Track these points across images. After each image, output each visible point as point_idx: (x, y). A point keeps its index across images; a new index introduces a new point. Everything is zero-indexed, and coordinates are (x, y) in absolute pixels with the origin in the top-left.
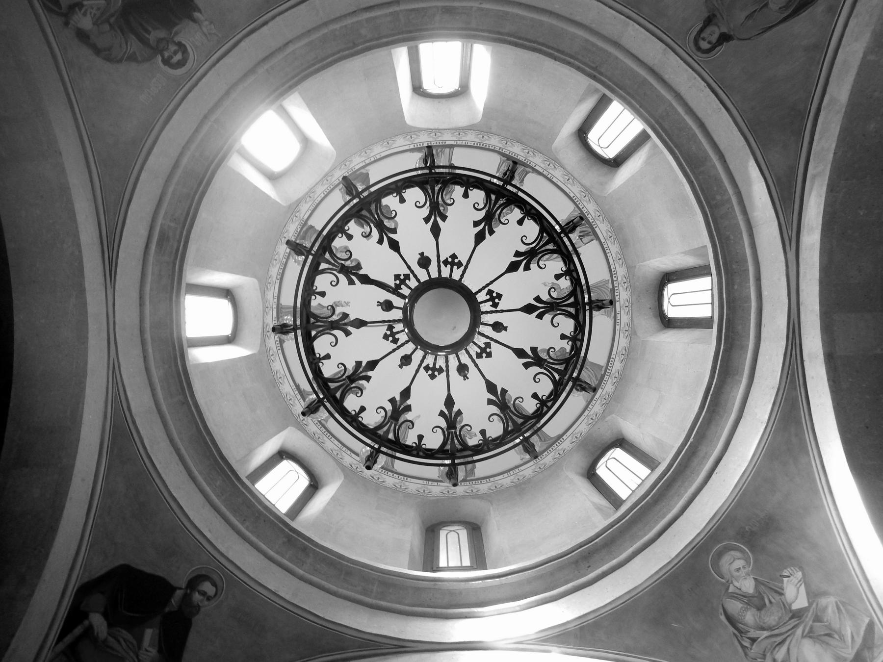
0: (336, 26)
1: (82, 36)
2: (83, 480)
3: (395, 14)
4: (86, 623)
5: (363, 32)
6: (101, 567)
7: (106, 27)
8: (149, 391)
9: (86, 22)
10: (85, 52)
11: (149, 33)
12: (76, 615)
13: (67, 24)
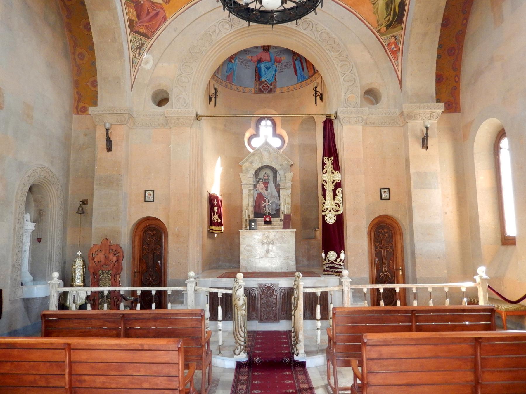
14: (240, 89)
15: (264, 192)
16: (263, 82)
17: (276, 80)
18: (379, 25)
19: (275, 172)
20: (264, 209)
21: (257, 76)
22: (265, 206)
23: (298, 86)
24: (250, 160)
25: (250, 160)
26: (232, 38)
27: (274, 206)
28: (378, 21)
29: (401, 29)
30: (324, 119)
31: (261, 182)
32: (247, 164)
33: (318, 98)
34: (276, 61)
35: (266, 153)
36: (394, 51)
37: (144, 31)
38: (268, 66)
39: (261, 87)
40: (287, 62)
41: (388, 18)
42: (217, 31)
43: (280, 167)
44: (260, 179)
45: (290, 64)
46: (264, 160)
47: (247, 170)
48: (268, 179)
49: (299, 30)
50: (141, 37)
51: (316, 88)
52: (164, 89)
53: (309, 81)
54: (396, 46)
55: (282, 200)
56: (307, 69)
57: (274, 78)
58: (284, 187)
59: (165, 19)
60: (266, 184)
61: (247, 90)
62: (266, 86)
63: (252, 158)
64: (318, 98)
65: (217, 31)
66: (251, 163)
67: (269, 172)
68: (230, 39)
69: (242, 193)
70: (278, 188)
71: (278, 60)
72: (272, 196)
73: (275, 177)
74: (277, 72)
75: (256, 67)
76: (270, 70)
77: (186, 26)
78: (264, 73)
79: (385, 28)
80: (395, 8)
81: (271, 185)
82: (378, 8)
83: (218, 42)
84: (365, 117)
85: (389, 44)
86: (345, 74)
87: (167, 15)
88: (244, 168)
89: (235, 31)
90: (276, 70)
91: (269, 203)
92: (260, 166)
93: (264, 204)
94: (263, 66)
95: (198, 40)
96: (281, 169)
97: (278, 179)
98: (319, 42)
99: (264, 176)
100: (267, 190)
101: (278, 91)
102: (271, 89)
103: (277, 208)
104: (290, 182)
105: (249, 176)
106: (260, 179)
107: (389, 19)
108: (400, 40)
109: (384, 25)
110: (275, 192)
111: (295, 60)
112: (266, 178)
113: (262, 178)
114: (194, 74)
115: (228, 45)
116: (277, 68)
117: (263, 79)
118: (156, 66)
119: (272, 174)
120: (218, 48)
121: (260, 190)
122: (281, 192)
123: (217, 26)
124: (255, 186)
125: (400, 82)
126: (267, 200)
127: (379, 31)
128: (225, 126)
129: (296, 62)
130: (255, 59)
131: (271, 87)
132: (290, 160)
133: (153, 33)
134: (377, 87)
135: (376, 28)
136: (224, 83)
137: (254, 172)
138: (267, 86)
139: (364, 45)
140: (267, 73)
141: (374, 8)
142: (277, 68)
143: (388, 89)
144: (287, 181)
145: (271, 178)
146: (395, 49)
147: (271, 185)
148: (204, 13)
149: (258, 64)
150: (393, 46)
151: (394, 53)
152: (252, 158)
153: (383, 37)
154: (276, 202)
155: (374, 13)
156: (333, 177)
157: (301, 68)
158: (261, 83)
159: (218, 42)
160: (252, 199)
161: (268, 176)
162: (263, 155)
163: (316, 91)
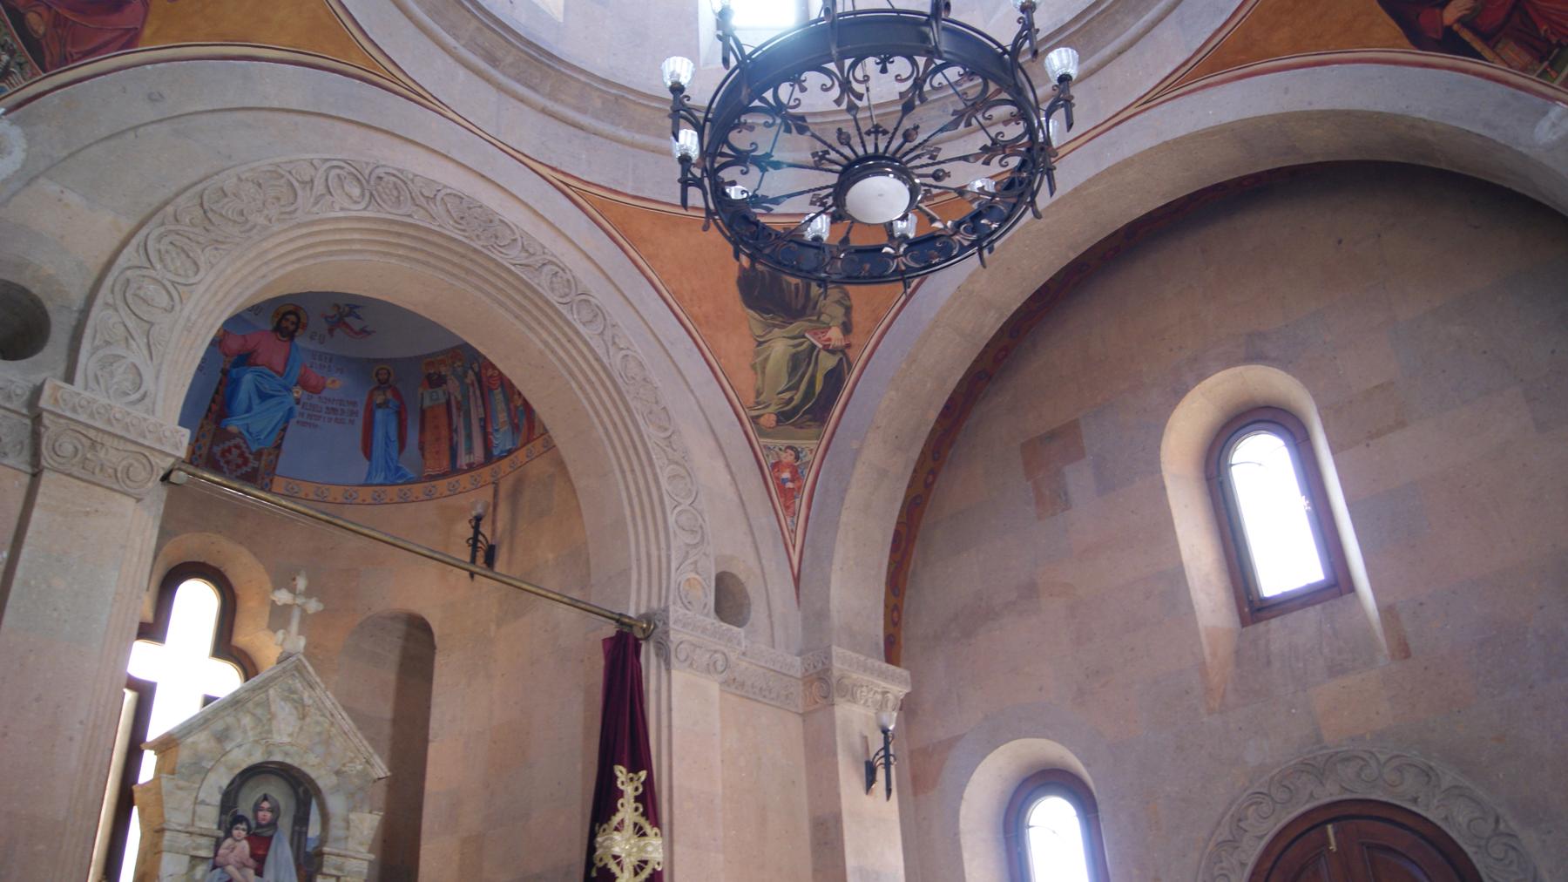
0: (623, 133)
1: (847, 328)
2: (1286, 91)
3: (552, 96)
4: (1456, 27)
5: (598, 103)
6: (1387, 26)
7: (824, 318)
8: (1156, 31)
9: (835, 335)
10: (856, 317)
11: (797, 286)
12: (1450, 43)
13: (848, 346)
16: (234, 436)
17: (278, 447)
18: (758, 403)
21: (216, 408)
23: (366, 493)
24: (219, 725)
26: (356, 236)
28: (759, 393)
29: (819, 437)
30: (610, 630)
31: (240, 831)
34: (303, 383)
35: (288, 707)
36: (785, 487)
37: (41, 30)
38: (267, 387)
39: (217, 450)
41: (787, 395)
42: (319, 187)
43: (334, 779)
44: (239, 819)
46: (277, 738)
48: (273, 824)
49: (569, 317)
50: (18, 44)
51: (478, 519)
52: (35, 291)
53: (418, 489)
54: (796, 475)
56: (422, 448)
57: (274, 437)
58: (340, 868)
59: (130, 40)
60: (260, 845)
62: (235, 452)
63: (230, 720)
65: (319, 187)
67: (278, 792)
68: (348, 236)
73: (301, 820)
74: (293, 421)
75: (225, 372)
77: (199, 108)
78: (244, 406)
79: (773, 418)
80: (813, 377)
81: (282, 852)
82: (766, 359)
83: (313, 223)
84: (733, 657)
85: (776, 466)
86: (680, 504)
87: (147, 32)
89: (375, 220)
90: (291, 410)
92: (258, 757)
94: (248, 380)
95: (240, 179)
96: (336, 789)
98: (619, 381)
99: (257, 808)
100: (259, 873)
101: (279, 484)
102: (255, 470)
104: (364, 849)
106: (239, 819)
107: (791, 399)
108: (809, 464)
109: (772, 408)
111: (379, 406)
112: (265, 816)
113: (249, 815)
114: (202, 288)
115: (331, 253)
116: (298, 408)
117: (234, 426)
118: (28, 184)
119: (292, 804)
120: (301, 243)
121: (231, 869)
123: (321, 171)
125: (797, 580)
127: (755, 420)
131: (253, 464)
133: (65, 61)
134: (742, 577)
135: (750, 408)
138: (242, 455)
139: (717, 440)
141: (757, 354)
142: (298, 408)
143: (770, 589)
144: (352, 844)
145: (285, 823)
146: (790, 485)
148: (276, 105)
149: (236, 365)
150: (786, 475)
151: (788, 496)
153: (763, 441)
155: (753, 367)
156: (642, 849)
158: (221, 434)
159: (313, 223)
161: (275, 810)
162: (273, 716)
163: (477, 532)
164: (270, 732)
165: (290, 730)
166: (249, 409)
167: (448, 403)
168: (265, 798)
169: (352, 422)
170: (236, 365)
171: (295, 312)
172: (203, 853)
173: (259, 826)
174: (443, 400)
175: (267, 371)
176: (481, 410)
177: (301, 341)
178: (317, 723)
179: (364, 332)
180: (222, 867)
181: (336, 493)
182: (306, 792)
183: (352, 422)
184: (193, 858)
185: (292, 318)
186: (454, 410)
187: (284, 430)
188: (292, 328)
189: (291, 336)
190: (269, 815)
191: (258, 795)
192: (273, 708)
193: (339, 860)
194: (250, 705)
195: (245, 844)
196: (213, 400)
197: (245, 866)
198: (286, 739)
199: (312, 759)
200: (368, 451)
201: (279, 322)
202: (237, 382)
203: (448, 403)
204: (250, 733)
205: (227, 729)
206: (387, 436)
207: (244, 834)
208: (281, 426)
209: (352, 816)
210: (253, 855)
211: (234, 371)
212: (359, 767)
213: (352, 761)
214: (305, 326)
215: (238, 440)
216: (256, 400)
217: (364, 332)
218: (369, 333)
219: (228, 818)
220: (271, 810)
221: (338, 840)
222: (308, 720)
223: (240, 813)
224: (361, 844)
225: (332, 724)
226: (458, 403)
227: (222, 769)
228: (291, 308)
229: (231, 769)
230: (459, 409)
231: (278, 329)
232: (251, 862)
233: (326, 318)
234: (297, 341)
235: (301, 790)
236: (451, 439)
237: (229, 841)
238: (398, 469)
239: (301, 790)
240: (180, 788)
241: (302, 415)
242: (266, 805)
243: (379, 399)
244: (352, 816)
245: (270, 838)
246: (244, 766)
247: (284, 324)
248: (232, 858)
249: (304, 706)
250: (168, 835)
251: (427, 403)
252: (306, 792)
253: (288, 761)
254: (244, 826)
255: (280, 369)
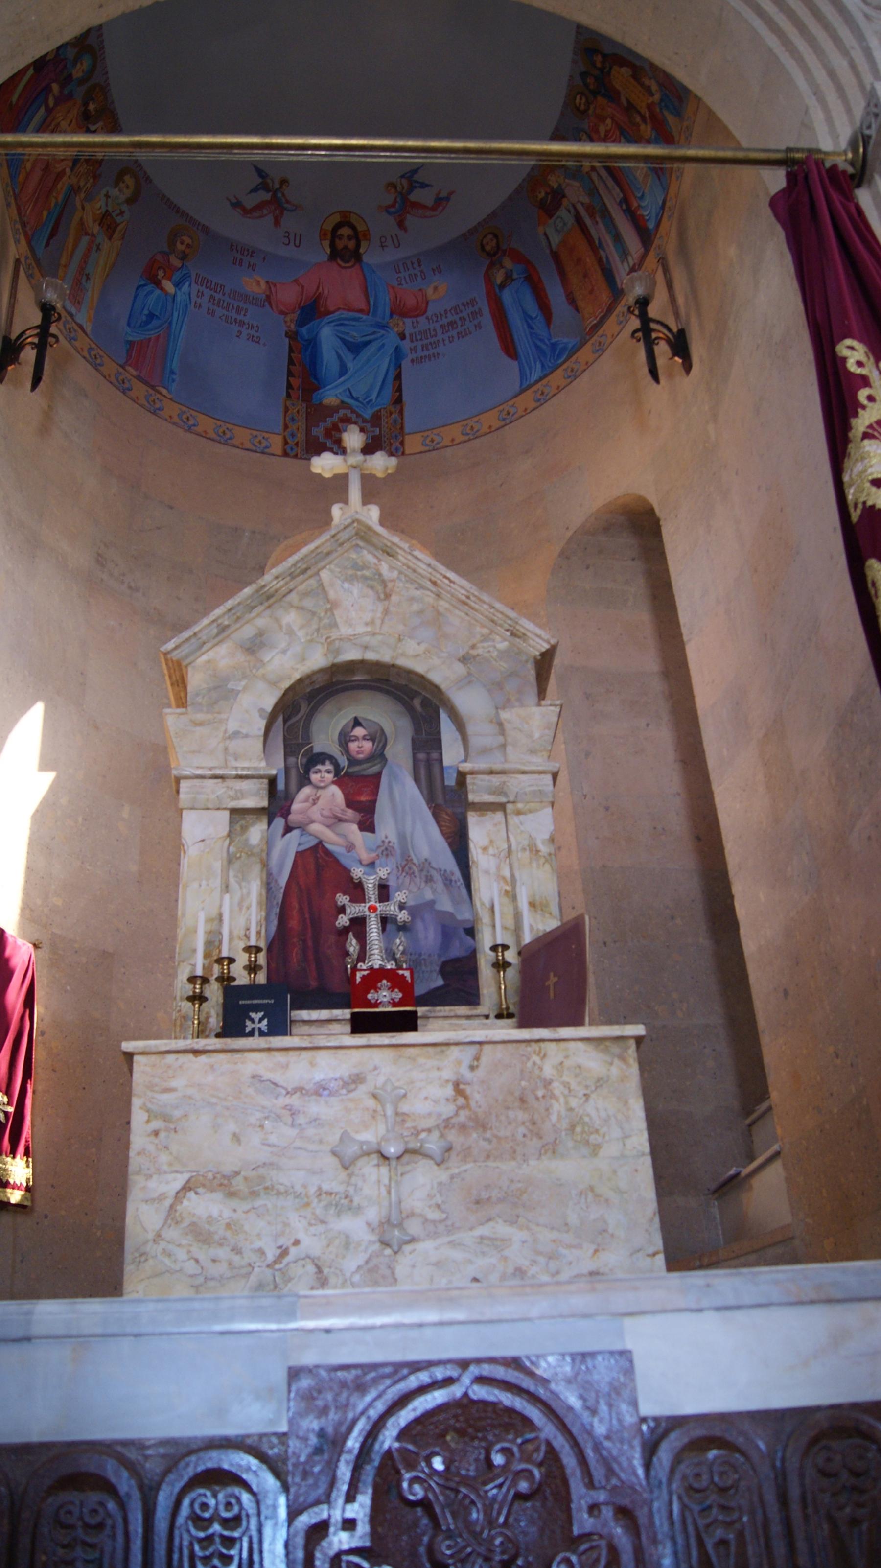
14: (206, 423)
15: (350, 843)
16: (334, 410)
17: (398, 401)
19: (421, 704)
20: (353, 945)
21: (296, 382)
22: (359, 925)
23: (527, 400)
24: (247, 632)
25: (247, 632)
27: (428, 937)
31: (323, 774)
32: (222, 656)
33: (662, 350)
34: (399, 311)
35: (356, 589)
38: (356, 336)
40: (456, 309)
43: (460, 669)
45: (474, 314)
46: (345, 630)
47: (222, 692)
48: (379, 756)
53: (585, 353)
55: (486, 888)
56: (572, 300)
57: (389, 391)
58: (500, 791)
60: (362, 793)
61: (242, 435)
63: (261, 622)
64: (662, 350)
66: (254, 647)
67: (379, 712)
69: (177, 847)
70: (452, 809)
71: (411, 302)
72: (406, 866)
73: (427, 742)
74: (406, 364)
75: (292, 336)
76: (366, 353)
78: (335, 367)
81: (402, 800)
88: (196, 680)
90: (398, 354)
91: (391, 908)
93: (354, 910)
96: (467, 681)
97: (452, 754)
99: (345, 739)
100: (367, 825)
103: (456, 951)
105: (232, 726)
110: (429, 841)
111: (502, 286)
112: (362, 747)
113: (335, 750)
116: (406, 345)
121: (315, 828)
122: (479, 831)
124: (278, 804)
126: (370, 885)
128: (100, 560)
129: (507, 296)
130: (288, 295)
132: (527, 625)
136: (111, 367)
137: (269, 702)
140: (350, 365)
142: (406, 345)
145: (400, 752)
147: (402, 800)
149: (303, 321)
152: (261, 622)
154: (445, 905)
157: (533, 309)
160: (255, 888)
161: (378, 737)
162: (333, 605)
163: (645, 320)
164: (334, 625)
165: (368, 617)
166: (343, 370)
167: (578, 219)
168: (357, 723)
169: (478, 326)
170: (303, 321)
171: (345, 221)
172: (249, 803)
173: (353, 761)
174: (570, 220)
175: (346, 314)
176: (617, 190)
177: (371, 256)
178: (412, 599)
179: (440, 201)
180: (302, 827)
181: (491, 419)
182: (425, 703)
183: (478, 326)
184: (234, 811)
185: (345, 231)
186: (588, 221)
187: (398, 377)
188: (352, 244)
189: (357, 256)
190: (368, 745)
191: (343, 719)
192: (332, 595)
193: (496, 780)
194: (293, 597)
195: (335, 790)
196: (290, 374)
197: (340, 820)
198: (361, 629)
199: (411, 647)
200: (510, 349)
201: (332, 245)
202: (313, 344)
203: (578, 219)
204: (301, 634)
205: (261, 634)
206: (527, 317)
207: (330, 777)
208: (391, 377)
209: (505, 715)
210: (350, 803)
211: (304, 330)
212: (503, 646)
213: (485, 638)
214: (366, 235)
215: (342, 412)
216: (348, 357)
217: (440, 201)
218: (448, 199)
219: (300, 760)
220: (371, 738)
221: (485, 751)
222: (394, 598)
223: (317, 749)
224: (533, 752)
225: (438, 596)
226: (589, 208)
227: (261, 685)
228: (337, 219)
229: (273, 684)
230: (592, 216)
231: (335, 255)
232: (350, 813)
233: (387, 209)
234: (366, 259)
235: (417, 703)
236: (600, 261)
237: (307, 791)
238: (554, 346)
239: (417, 703)
240: (201, 724)
241: (414, 350)
242: (359, 732)
243: (499, 278)
244: (505, 715)
245: (378, 776)
246: (297, 676)
247: (340, 244)
248: (315, 812)
249: (384, 583)
250: (184, 785)
251: (555, 240)
252: (425, 703)
253: (371, 656)
254: (328, 766)
255: (362, 305)
